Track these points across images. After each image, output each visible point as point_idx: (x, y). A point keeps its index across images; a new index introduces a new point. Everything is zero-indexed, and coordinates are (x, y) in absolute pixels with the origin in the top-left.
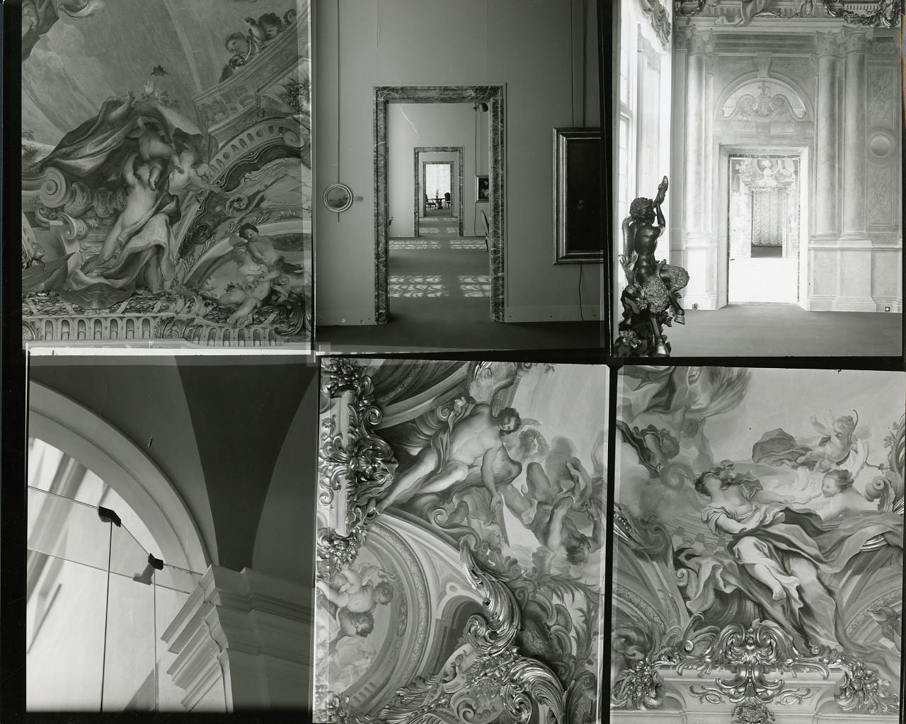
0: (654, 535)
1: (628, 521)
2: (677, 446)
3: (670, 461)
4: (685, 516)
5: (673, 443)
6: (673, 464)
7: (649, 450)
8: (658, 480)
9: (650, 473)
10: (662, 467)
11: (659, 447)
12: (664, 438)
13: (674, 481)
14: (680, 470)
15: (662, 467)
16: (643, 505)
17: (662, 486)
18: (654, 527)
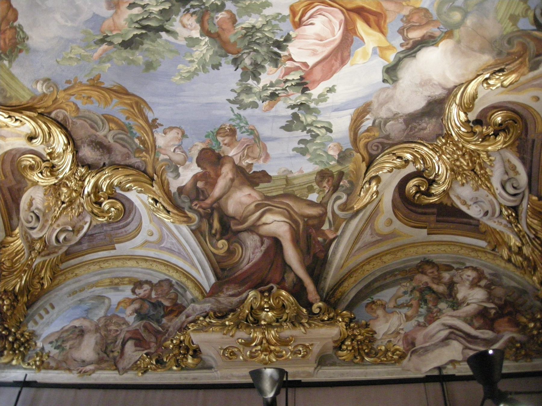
0: (515, 46)
1: (496, 69)
2: (419, 10)
3: (435, 17)
4: (496, 11)
5: (415, 13)
6: (439, 14)
7: (424, 36)
8: (456, 32)
9: (448, 38)
10: (441, 26)
11: (420, 26)
12: (411, 21)
13: (457, 16)
14: (445, 8)
15: (441, 26)
16: (482, 50)
17: (462, 28)
18: (506, 45)
